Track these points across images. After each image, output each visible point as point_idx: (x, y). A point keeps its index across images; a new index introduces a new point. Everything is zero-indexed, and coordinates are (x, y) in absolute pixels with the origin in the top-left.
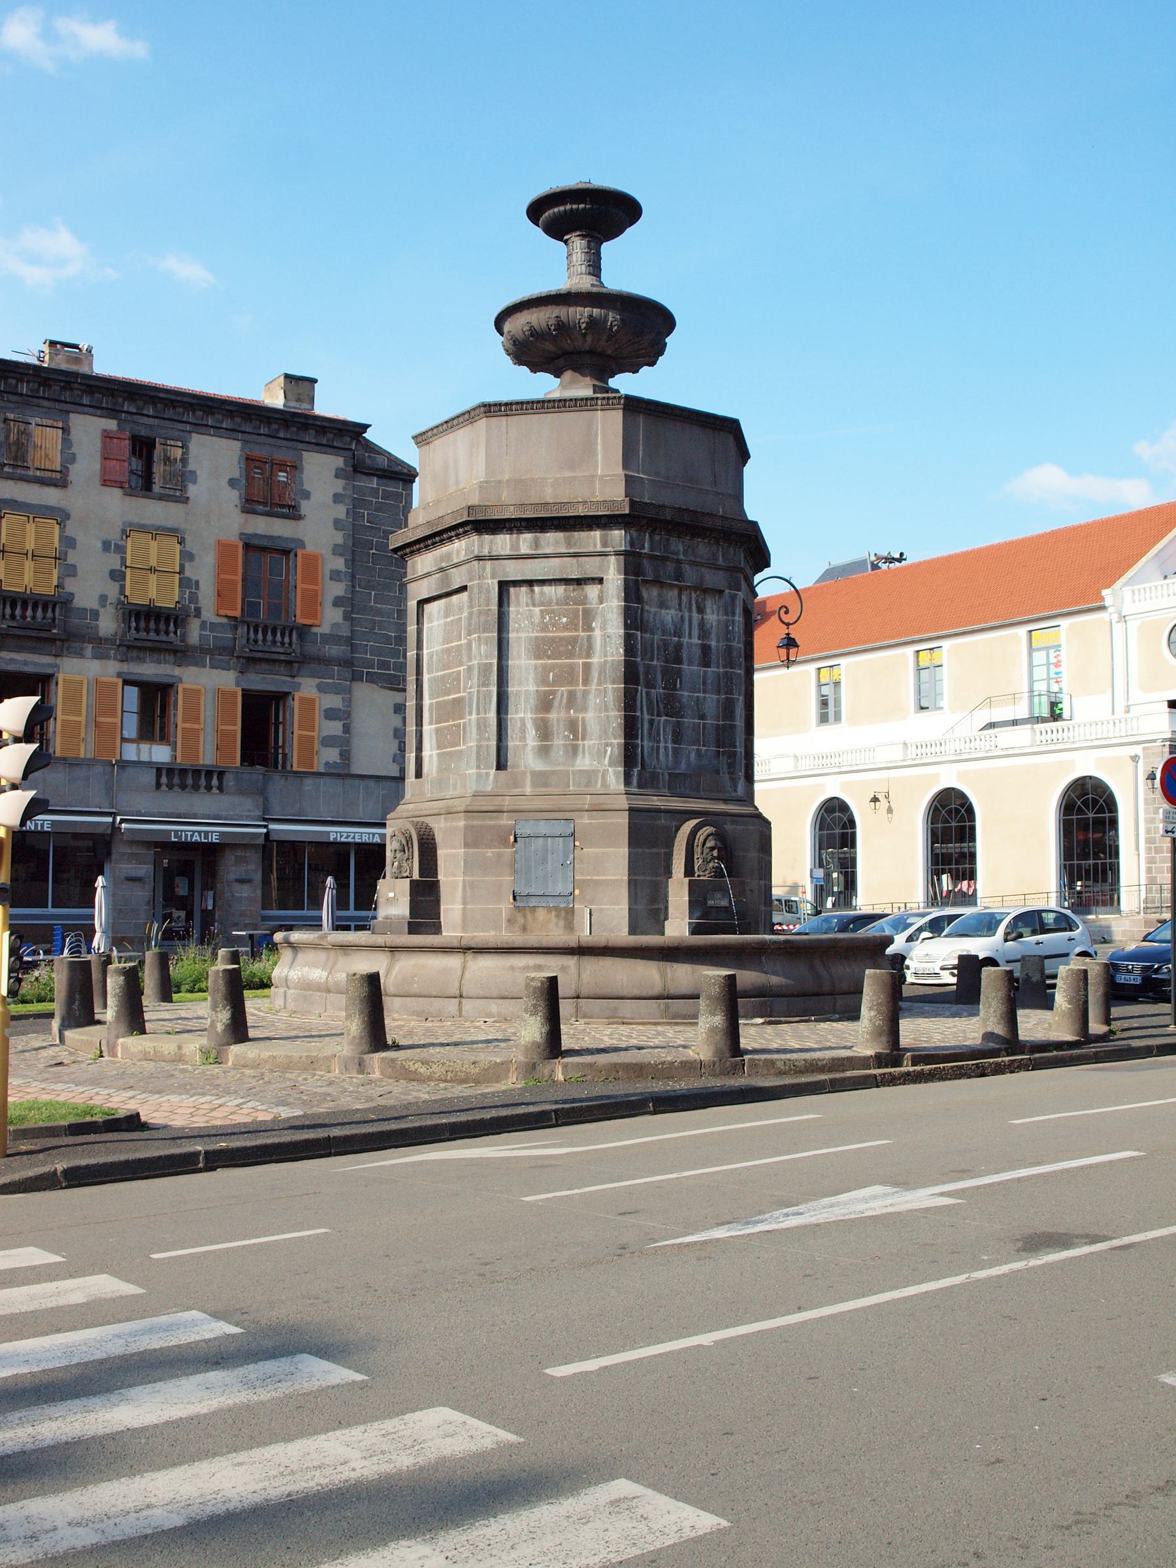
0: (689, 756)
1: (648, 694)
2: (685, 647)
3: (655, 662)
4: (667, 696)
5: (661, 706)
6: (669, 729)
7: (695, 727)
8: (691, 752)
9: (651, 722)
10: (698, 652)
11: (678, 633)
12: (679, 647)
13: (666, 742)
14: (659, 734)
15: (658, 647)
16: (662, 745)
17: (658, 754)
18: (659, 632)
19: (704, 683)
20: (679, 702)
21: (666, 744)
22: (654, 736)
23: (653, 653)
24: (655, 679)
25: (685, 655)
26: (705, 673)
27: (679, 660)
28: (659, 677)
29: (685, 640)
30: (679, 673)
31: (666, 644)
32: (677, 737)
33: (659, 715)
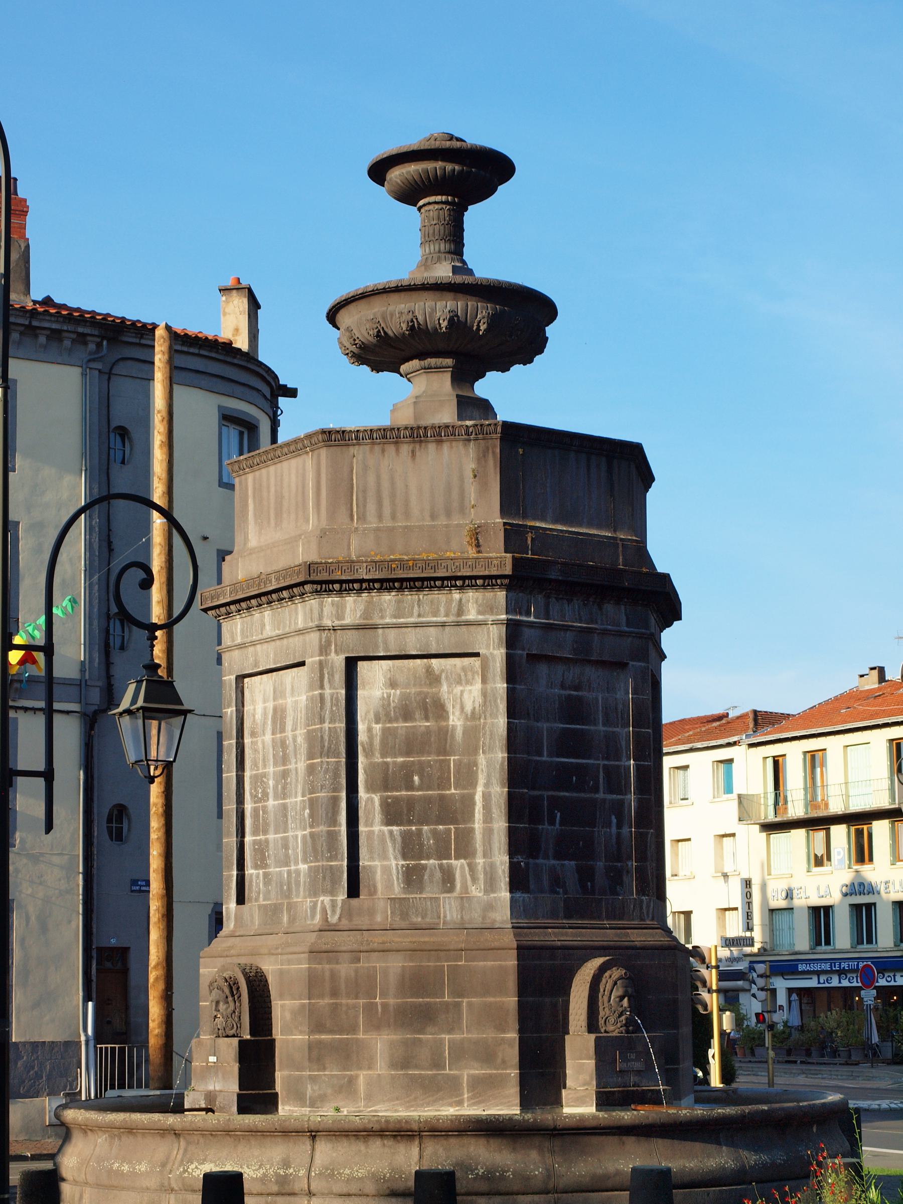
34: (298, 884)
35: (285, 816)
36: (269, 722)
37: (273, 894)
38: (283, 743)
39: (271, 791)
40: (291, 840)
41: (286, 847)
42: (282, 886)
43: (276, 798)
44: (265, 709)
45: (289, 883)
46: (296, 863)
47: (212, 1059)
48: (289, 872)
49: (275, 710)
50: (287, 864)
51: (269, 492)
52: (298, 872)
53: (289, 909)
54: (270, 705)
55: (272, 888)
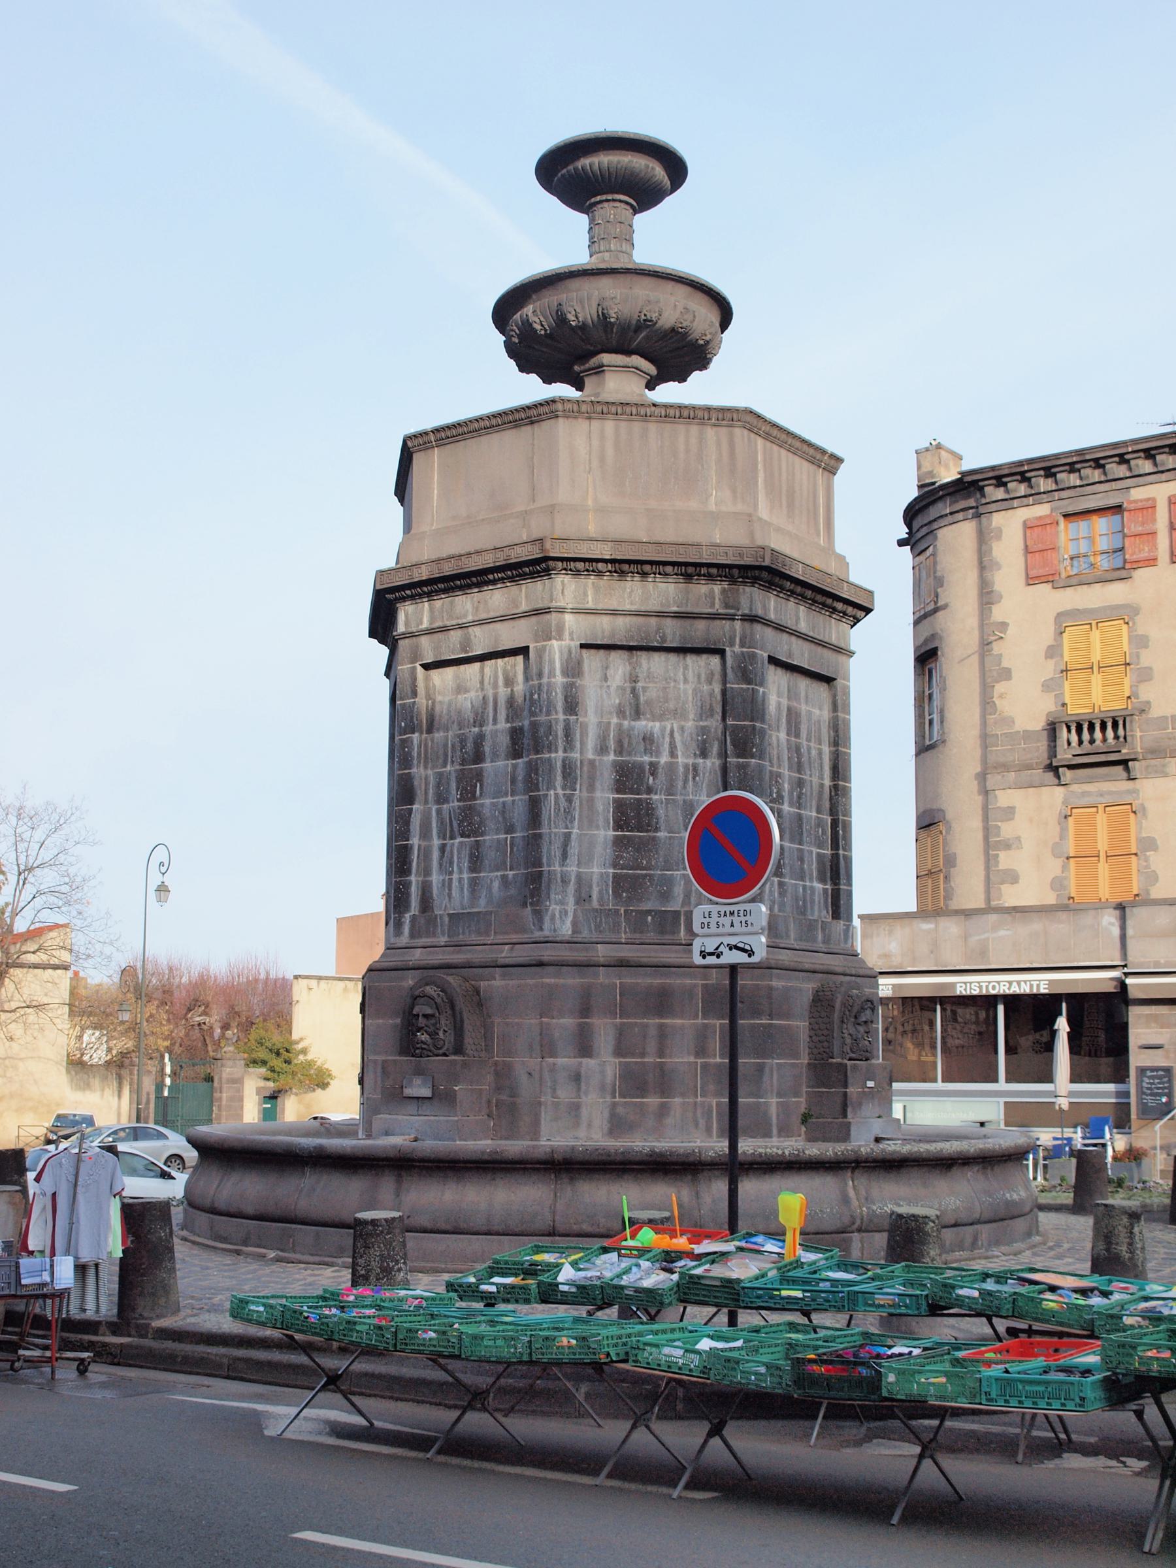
0: (490, 889)
1: (439, 812)
2: (488, 737)
3: (449, 768)
4: (463, 809)
5: (455, 824)
6: (465, 853)
7: (500, 845)
8: (493, 879)
9: (443, 849)
10: (504, 741)
11: (479, 721)
12: (480, 739)
13: (461, 872)
14: (451, 863)
15: (453, 746)
16: (455, 876)
17: (450, 889)
18: (455, 726)
19: (513, 781)
20: (479, 816)
21: (461, 875)
22: (446, 867)
23: (446, 755)
24: (448, 791)
25: (487, 749)
26: (515, 767)
27: (479, 757)
28: (453, 785)
29: (488, 728)
30: (479, 776)
31: (462, 740)
32: (476, 862)
33: (452, 838)
34: (813, 902)
35: (800, 827)
36: (784, 720)
37: (788, 909)
38: (798, 749)
39: (786, 794)
40: (806, 854)
41: (801, 859)
42: (797, 900)
43: (791, 804)
44: (779, 704)
45: (804, 901)
46: (811, 880)
47: (870, 1084)
48: (804, 887)
49: (789, 709)
50: (802, 879)
51: (780, 474)
52: (812, 889)
53: (823, 929)
54: (785, 702)
55: (788, 899)
